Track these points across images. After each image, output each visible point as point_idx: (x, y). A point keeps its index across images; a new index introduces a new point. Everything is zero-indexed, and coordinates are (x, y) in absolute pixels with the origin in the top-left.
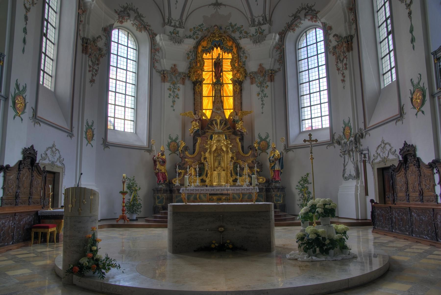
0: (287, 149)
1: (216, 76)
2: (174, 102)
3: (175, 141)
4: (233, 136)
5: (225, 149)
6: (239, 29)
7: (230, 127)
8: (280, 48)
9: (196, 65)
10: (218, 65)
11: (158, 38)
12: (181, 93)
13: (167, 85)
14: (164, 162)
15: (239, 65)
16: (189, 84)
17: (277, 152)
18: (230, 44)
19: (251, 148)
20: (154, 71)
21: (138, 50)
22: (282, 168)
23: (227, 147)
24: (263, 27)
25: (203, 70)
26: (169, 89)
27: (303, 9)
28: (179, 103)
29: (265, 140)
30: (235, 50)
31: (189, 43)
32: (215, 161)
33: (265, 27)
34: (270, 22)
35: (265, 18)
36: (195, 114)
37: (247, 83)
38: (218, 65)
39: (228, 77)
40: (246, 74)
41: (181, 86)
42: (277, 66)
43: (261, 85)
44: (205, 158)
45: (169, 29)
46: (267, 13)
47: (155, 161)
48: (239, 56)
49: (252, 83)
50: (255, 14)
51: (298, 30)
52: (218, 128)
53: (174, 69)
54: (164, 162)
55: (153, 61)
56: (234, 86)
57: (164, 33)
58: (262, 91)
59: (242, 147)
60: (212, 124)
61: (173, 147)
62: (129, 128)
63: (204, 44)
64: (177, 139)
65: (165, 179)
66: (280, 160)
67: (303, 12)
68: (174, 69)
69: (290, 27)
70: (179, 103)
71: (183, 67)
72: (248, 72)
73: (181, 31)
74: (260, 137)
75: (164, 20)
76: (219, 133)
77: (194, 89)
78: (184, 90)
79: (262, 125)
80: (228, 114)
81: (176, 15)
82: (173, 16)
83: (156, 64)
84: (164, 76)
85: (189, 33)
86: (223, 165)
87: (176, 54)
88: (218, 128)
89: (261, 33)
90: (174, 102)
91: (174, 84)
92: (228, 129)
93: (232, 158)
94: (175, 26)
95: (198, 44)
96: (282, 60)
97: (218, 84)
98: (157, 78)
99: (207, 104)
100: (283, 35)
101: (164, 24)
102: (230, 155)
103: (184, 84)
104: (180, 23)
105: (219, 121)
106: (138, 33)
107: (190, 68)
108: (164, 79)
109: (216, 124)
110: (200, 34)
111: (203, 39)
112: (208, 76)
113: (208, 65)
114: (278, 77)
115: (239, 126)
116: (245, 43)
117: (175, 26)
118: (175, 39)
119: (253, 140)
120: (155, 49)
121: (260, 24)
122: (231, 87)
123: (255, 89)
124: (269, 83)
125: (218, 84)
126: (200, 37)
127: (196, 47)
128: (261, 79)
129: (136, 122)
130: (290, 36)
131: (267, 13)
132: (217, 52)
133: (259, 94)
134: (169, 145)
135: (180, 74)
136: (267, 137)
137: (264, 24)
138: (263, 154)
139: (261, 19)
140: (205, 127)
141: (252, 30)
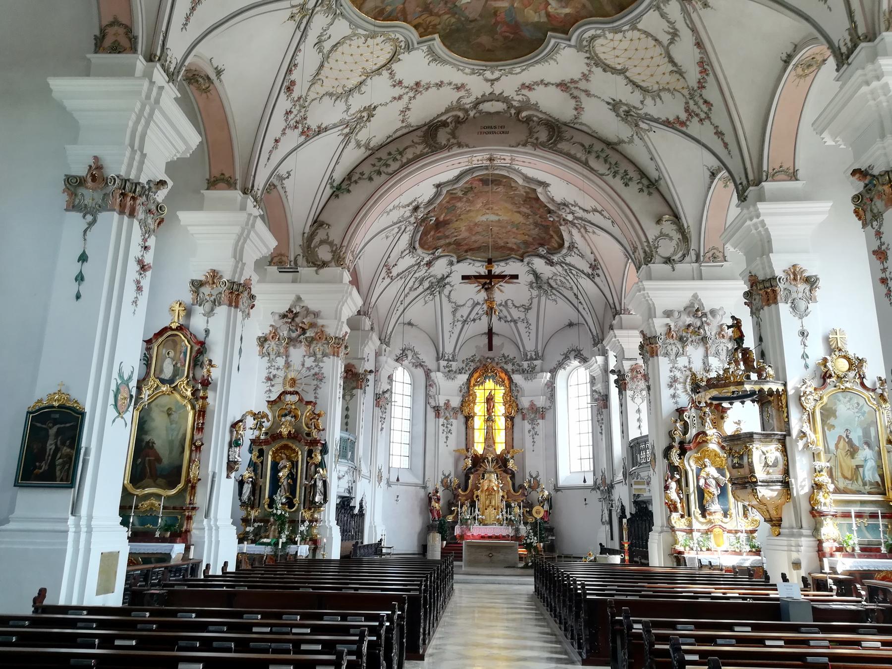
0: (557, 489)
1: (488, 410)
2: (447, 437)
3: (448, 477)
4: (505, 475)
5: (495, 488)
6: (512, 361)
7: (502, 462)
8: (551, 387)
9: (468, 397)
10: (490, 400)
11: (433, 375)
12: (454, 429)
13: (442, 420)
14: (438, 499)
15: (511, 399)
16: (461, 419)
17: (546, 493)
18: (503, 375)
19: (522, 487)
20: (428, 406)
21: (413, 384)
22: (550, 508)
23: (498, 486)
24: (535, 362)
25: (475, 403)
26: (443, 425)
27: (573, 350)
28: (452, 437)
29: (535, 478)
30: (507, 382)
31: (464, 377)
32: (486, 499)
33: (537, 363)
34: (542, 358)
35: (537, 354)
36: (467, 450)
37: (518, 419)
38: (490, 400)
39: (500, 409)
40: (519, 410)
41: (454, 422)
42: (548, 404)
43: (532, 421)
44: (477, 496)
45: (443, 363)
46: (540, 348)
47: (430, 499)
48: (511, 390)
49: (523, 419)
50: (528, 348)
51: (568, 369)
52: (489, 467)
53: (447, 404)
54: (438, 499)
55: (427, 396)
56: (506, 421)
57: (439, 371)
58: (533, 428)
59: (513, 485)
60: (484, 462)
61: (446, 486)
62: (405, 463)
63: (476, 375)
64: (449, 475)
65: (438, 514)
66: (549, 500)
67: (573, 354)
68: (447, 404)
69: (560, 365)
70: (452, 437)
71: (455, 402)
72: (520, 407)
73: (454, 364)
74: (531, 476)
75: (438, 354)
76: (491, 472)
77: (466, 423)
78: (457, 424)
79: (533, 464)
80: (500, 448)
81: (449, 349)
82: (446, 351)
83: (431, 400)
84: (437, 409)
85: (461, 365)
86: (493, 503)
87: (449, 389)
88: (489, 467)
89: (534, 368)
90: (447, 437)
91: (446, 418)
92: (500, 467)
93: (503, 496)
94: (448, 360)
95: (471, 375)
96: (552, 397)
97: (489, 419)
98: (431, 414)
99: (479, 437)
100: (554, 372)
101: (438, 359)
102: (501, 494)
103: (456, 419)
104: (453, 357)
105: (490, 459)
106: (413, 369)
107: (463, 403)
108: (438, 415)
109: (488, 462)
110: (473, 366)
111: (475, 370)
112: (480, 409)
113: (480, 394)
114: (548, 415)
115: (511, 464)
116: (517, 378)
117: (448, 360)
118: (450, 374)
119: (524, 478)
120: (429, 383)
121: (532, 359)
122: (503, 419)
123: (527, 426)
124: (540, 421)
125: (489, 419)
126: (472, 368)
127: (469, 380)
128: (533, 416)
129: (411, 457)
130: (561, 374)
131: (540, 348)
132: (489, 384)
133: (529, 431)
134: (442, 482)
135: (453, 409)
136: (537, 476)
137: (536, 359)
138: (534, 493)
139: (533, 353)
140: (478, 461)
141: (525, 364)
